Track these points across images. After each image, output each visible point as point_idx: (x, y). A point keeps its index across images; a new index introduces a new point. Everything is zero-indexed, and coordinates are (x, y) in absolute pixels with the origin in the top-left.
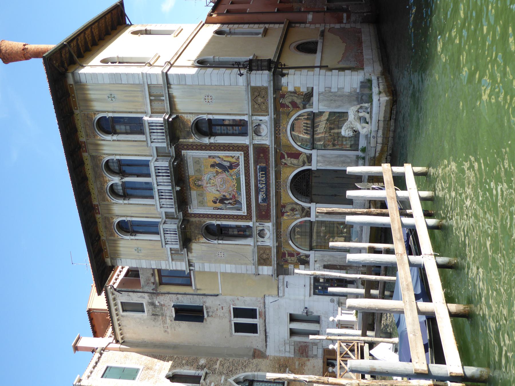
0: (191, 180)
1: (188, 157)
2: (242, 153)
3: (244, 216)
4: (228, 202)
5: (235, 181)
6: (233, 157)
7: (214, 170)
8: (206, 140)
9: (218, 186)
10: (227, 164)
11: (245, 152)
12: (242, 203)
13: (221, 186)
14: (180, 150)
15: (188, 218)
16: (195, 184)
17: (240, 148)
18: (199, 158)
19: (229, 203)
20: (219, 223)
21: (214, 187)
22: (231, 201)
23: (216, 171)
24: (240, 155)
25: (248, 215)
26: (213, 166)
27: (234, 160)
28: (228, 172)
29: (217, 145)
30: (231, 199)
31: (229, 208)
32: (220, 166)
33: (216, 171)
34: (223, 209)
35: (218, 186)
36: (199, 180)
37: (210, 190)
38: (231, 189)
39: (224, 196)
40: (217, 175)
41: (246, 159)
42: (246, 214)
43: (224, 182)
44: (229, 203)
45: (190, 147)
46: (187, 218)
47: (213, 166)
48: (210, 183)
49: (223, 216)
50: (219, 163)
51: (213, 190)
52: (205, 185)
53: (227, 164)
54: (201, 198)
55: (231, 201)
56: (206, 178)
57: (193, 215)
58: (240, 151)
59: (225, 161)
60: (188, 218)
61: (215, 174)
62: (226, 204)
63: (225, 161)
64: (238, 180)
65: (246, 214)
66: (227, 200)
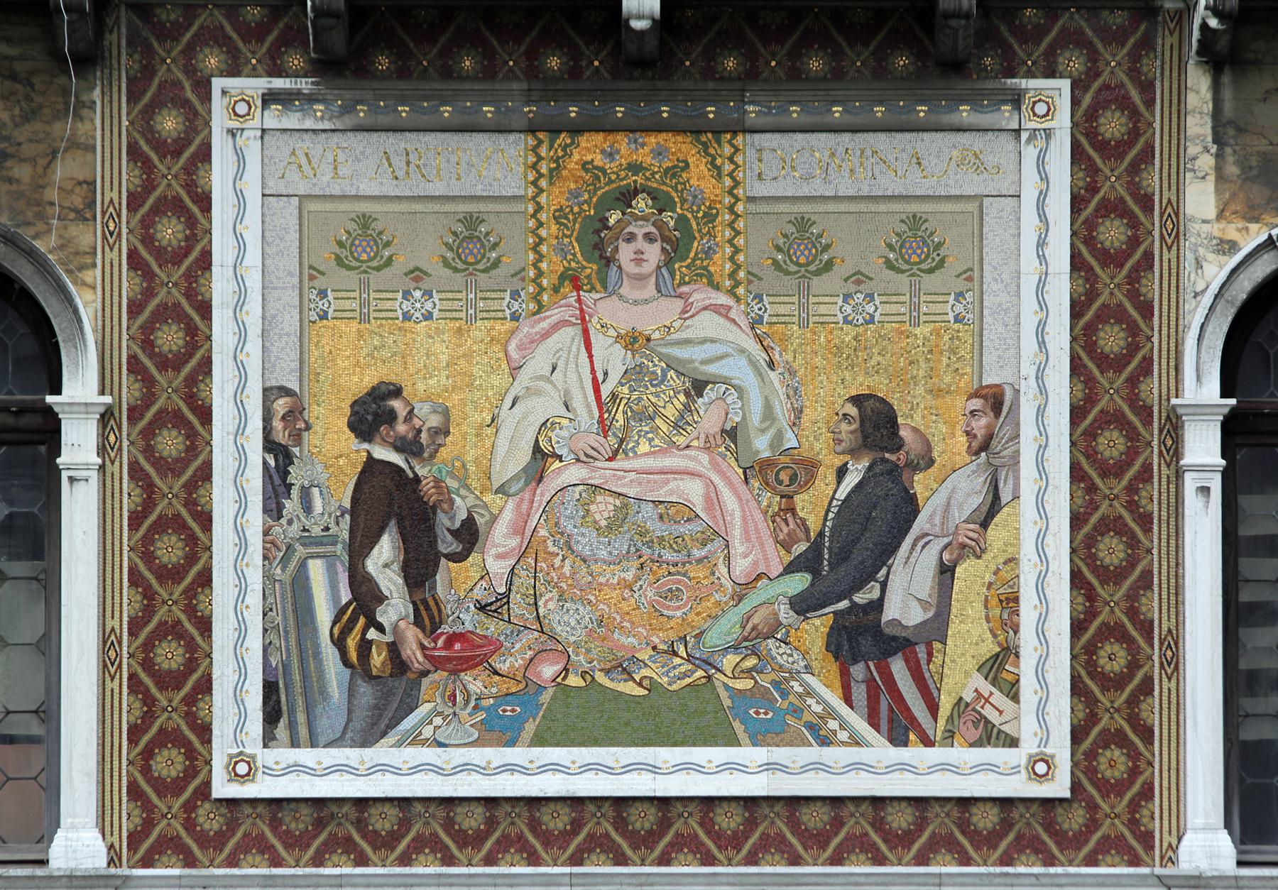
0: (679, 146)
1: (997, 149)
2: (1059, 787)
3: (197, 762)
4: (390, 581)
5: (673, 675)
6: (1000, 667)
7: (821, 431)
8: (1202, 387)
9: (601, 473)
10: (904, 595)
11: (1074, 820)
12: (381, 753)
13: (603, 508)
14: (1075, 62)
15: (125, 63)
16: (625, 198)
17: (1113, 763)
18: (969, 275)
19: (365, 598)
20: (79, 444)
21: (586, 414)
22: (396, 608)
23: (805, 470)
24: (1031, 754)
25: (209, 821)
26: (876, 424)
27: (959, 674)
28: (803, 605)
29: (1154, 497)
30: (427, 615)
31: (300, 584)
32: (880, 518)
33: (805, 470)
34: (273, 509)
35: (601, 473)
36: (676, 246)
37: (539, 362)
38: (569, 622)
39: (469, 535)
40: (757, 471)
41: (986, 820)
42: (222, 788)
43: (667, 544)
44: (365, 598)
45: (1113, 183)
46: (117, 39)
47: (876, 424)
48: (634, 375)
49: (170, 500)
50: (909, 507)
51: (546, 406)
52: (611, 313)
53: (904, 595)
54: (424, 247)
55: (396, 608)
56: (713, 332)
57: (169, 123)
58: (1084, 764)
59: (946, 572)
60: (125, 63)
61: (762, 445)
62: (360, 546)
63: (946, 572)
64: (691, 717)
65: (222, 788)
66: (419, 570)
